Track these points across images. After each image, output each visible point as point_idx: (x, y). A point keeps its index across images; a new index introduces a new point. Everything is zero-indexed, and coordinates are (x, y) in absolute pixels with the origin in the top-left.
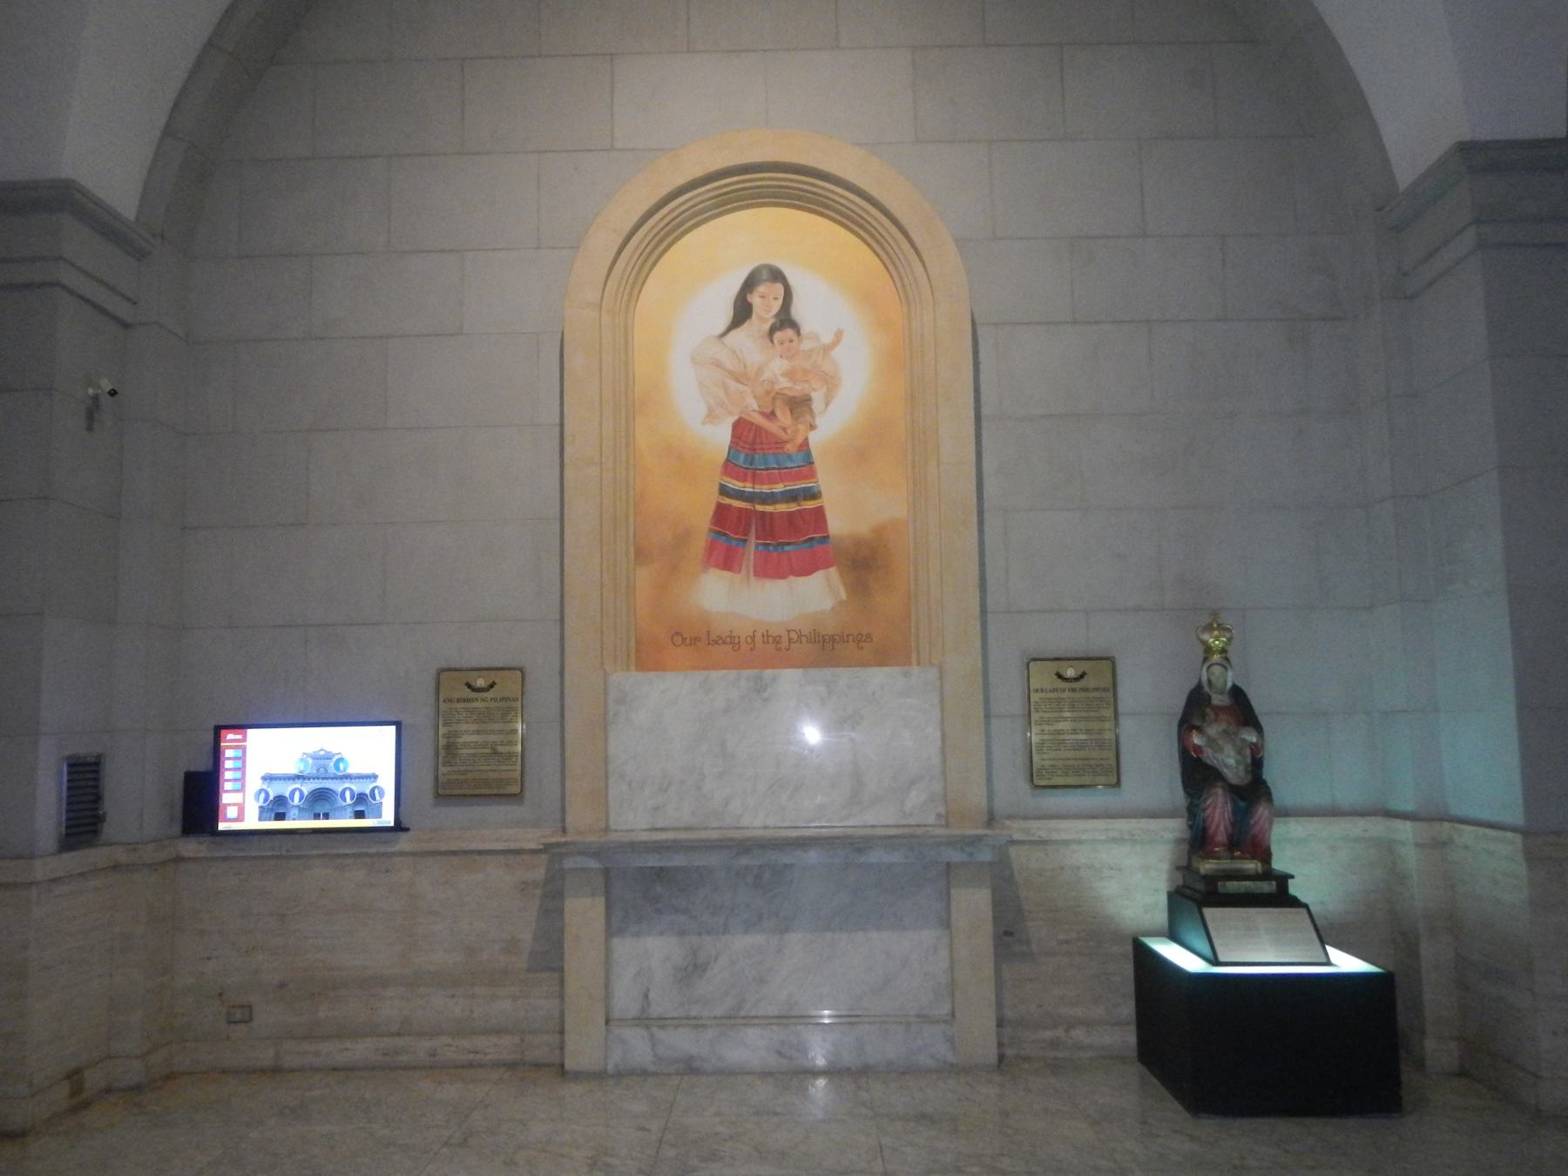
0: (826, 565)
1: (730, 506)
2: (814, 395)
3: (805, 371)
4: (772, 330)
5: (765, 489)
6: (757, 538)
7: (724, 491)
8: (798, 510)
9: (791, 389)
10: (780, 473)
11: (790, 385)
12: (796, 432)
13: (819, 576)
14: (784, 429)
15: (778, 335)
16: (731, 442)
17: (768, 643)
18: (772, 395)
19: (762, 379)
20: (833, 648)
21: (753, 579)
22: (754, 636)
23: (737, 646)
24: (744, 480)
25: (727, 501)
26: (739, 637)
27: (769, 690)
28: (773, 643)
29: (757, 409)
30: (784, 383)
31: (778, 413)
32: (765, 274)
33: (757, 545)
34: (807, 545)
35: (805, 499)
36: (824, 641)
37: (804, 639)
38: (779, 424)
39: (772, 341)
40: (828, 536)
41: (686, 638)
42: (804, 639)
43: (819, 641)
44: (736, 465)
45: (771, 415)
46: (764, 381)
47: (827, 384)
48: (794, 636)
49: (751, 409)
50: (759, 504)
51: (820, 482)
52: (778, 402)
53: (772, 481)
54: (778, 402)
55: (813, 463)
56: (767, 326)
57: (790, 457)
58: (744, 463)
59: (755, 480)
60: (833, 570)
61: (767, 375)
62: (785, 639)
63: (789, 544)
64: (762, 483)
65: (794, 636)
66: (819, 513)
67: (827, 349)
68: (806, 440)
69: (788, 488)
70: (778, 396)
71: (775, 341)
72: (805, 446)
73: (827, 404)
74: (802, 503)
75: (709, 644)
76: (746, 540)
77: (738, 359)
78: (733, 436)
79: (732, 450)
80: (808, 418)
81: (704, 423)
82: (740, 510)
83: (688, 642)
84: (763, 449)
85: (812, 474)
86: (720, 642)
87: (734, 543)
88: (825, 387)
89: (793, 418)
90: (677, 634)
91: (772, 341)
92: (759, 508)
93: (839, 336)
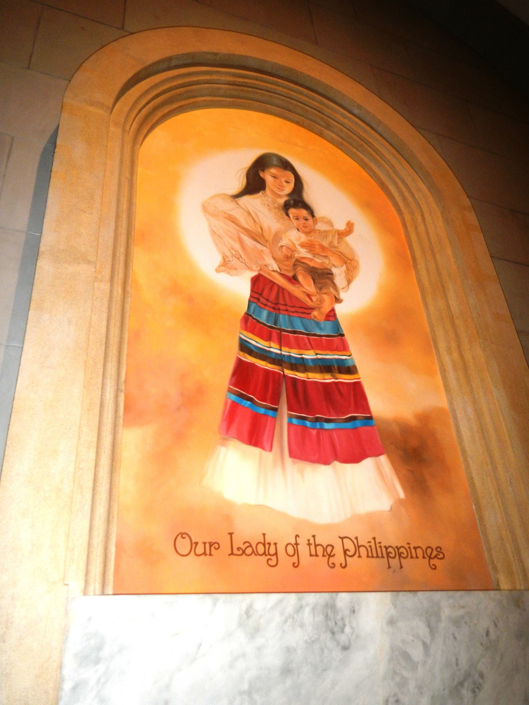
0: (377, 454)
1: (253, 365)
2: (334, 270)
3: (323, 248)
4: (286, 207)
5: (294, 353)
6: (290, 409)
7: (244, 347)
8: (334, 382)
9: (311, 260)
10: (309, 339)
11: (309, 256)
12: (321, 301)
13: (368, 463)
14: (309, 296)
15: (293, 212)
16: (251, 296)
17: (317, 555)
18: (293, 260)
19: (280, 244)
20: (401, 567)
21: (288, 460)
22: (297, 544)
23: (274, 558)
24: (268, 338)
25: (249, 359)
26: (275, 544)
27: (347, 630)
28: (324, 556)
29: (279, 270)
30: (303, 253)
31: (300, 278)
32: (275, 161)
33: (290, 417)
34: (349, 425)
35: (340, 372)
36: (388, 554)
37: (363, 551)
38: (303, 289)
39: (288, 215)
40: (371, 418)
41: (197, 543)
42: (363, 551)
43: (383, 557)
44: (258, 321)
45: (294, 280)
46: (282, 246)
47: (346, 263)
48: (349, 545)
49: (272, 269)
50: (288, 369)
51: (354, 356)
52: (299, 269)
53: (300, 346)
54: (299, 269)
55: (343, 335)
56: (282, 201)
57: (318, 324)
58: (268, 320)
59: (282, 342)
60: (383, 459)
61: (284, 242)
62: (338, 551)
63: (328, 421)
64: (291, 347)
65: (349, 545)
66: (357, 388)
67: (342, 235)
68: (333, 310)
69: (319, 357)
70: (298, 262)
71: (291, 216)
72: (331, 315)
73: (349, 282)
74: (338, 375)
75: (232, 554)
76: (276, 410)
77: (255, 221)
78: (252, 291)
79: (253, 306)
80: (332, 290)
81: (217, 271)
82: (267, 372)
83: (200, 549)
84: (287, 310)
85: (344, 347)
86: (249, 551)
87: (262, 411)
88: (345, 267)
89: (316, 287)
90: (183, 535)
91: (288, 215)
92: (288, 373)
93: (350, 228)
